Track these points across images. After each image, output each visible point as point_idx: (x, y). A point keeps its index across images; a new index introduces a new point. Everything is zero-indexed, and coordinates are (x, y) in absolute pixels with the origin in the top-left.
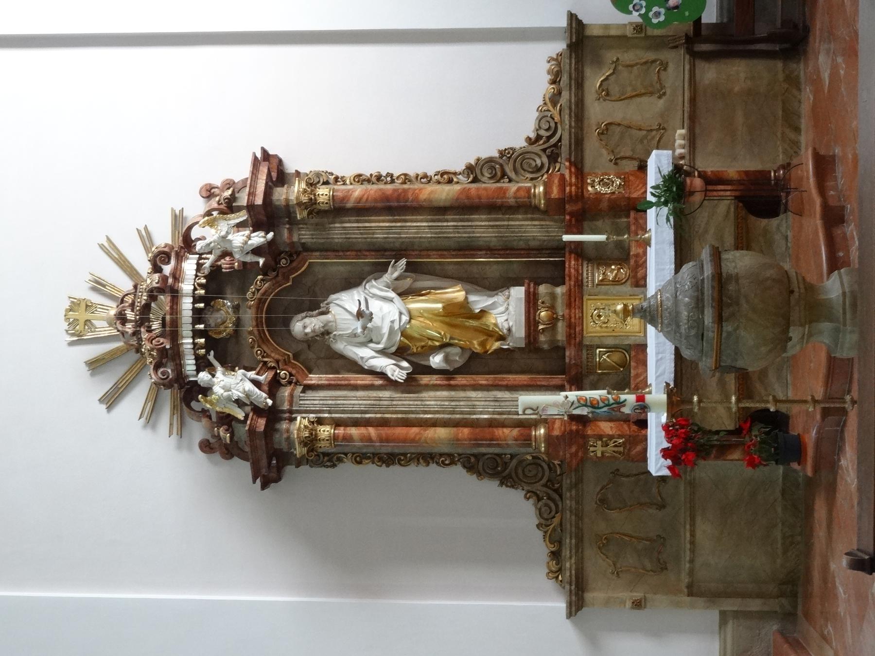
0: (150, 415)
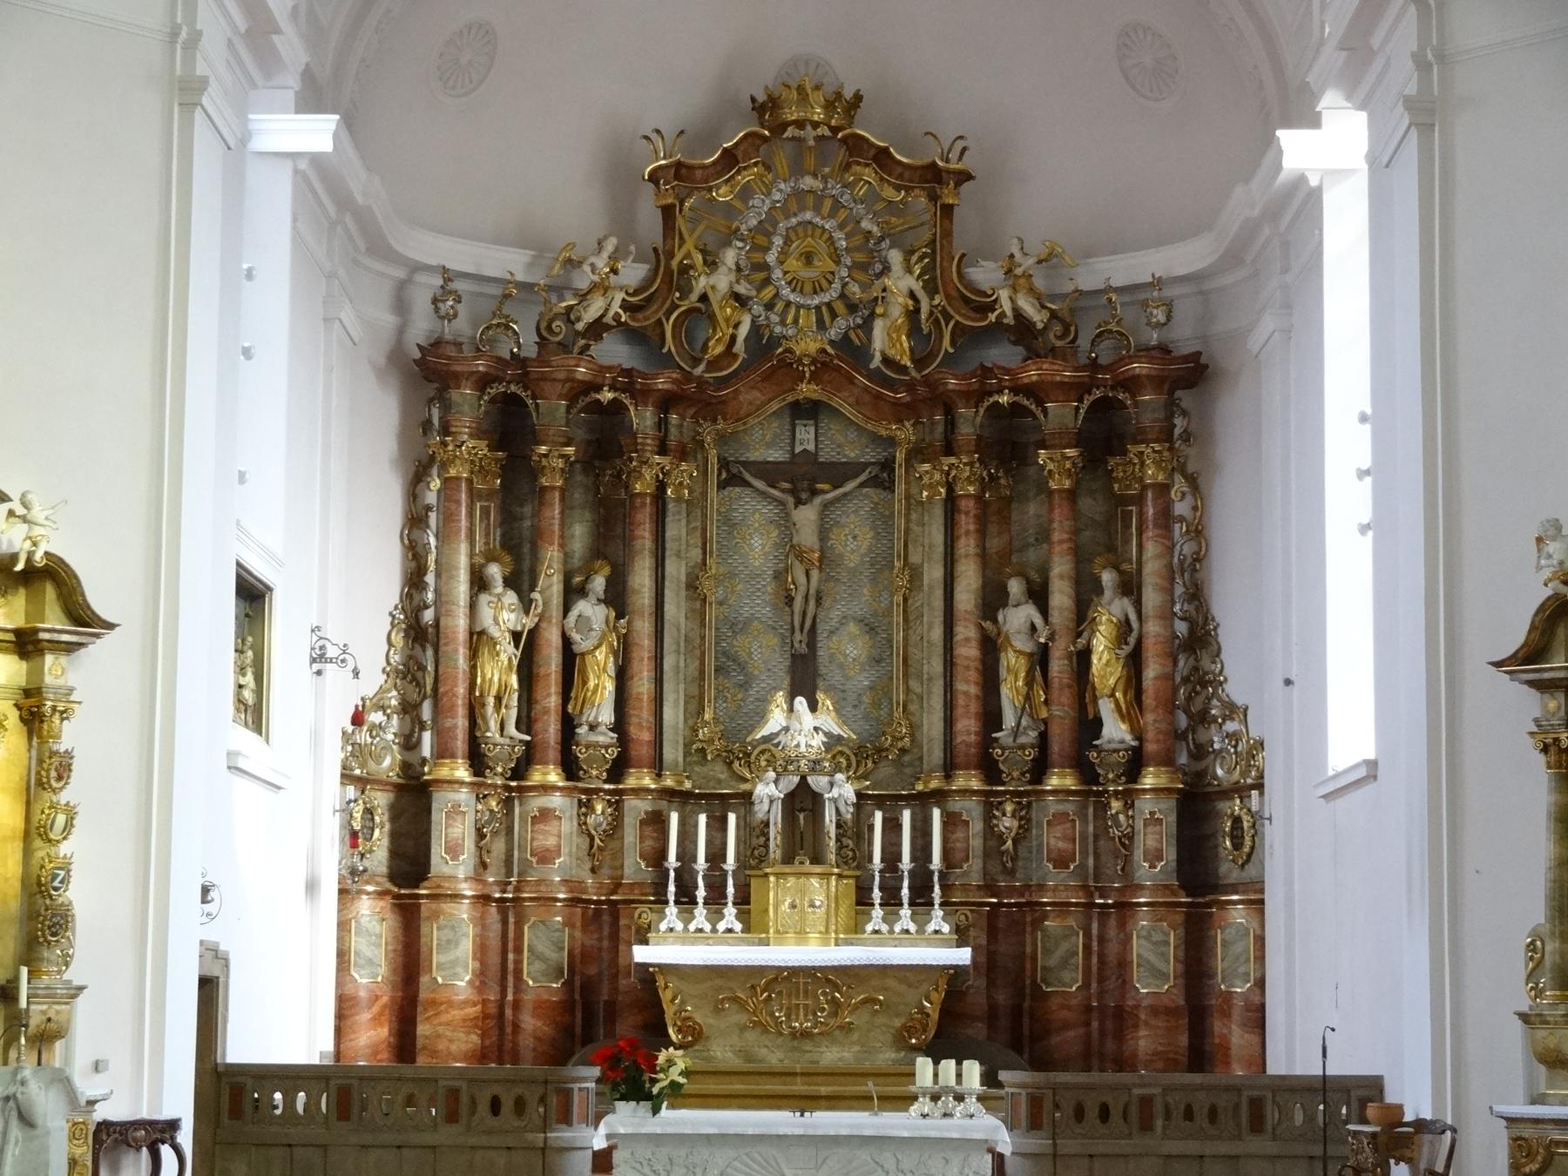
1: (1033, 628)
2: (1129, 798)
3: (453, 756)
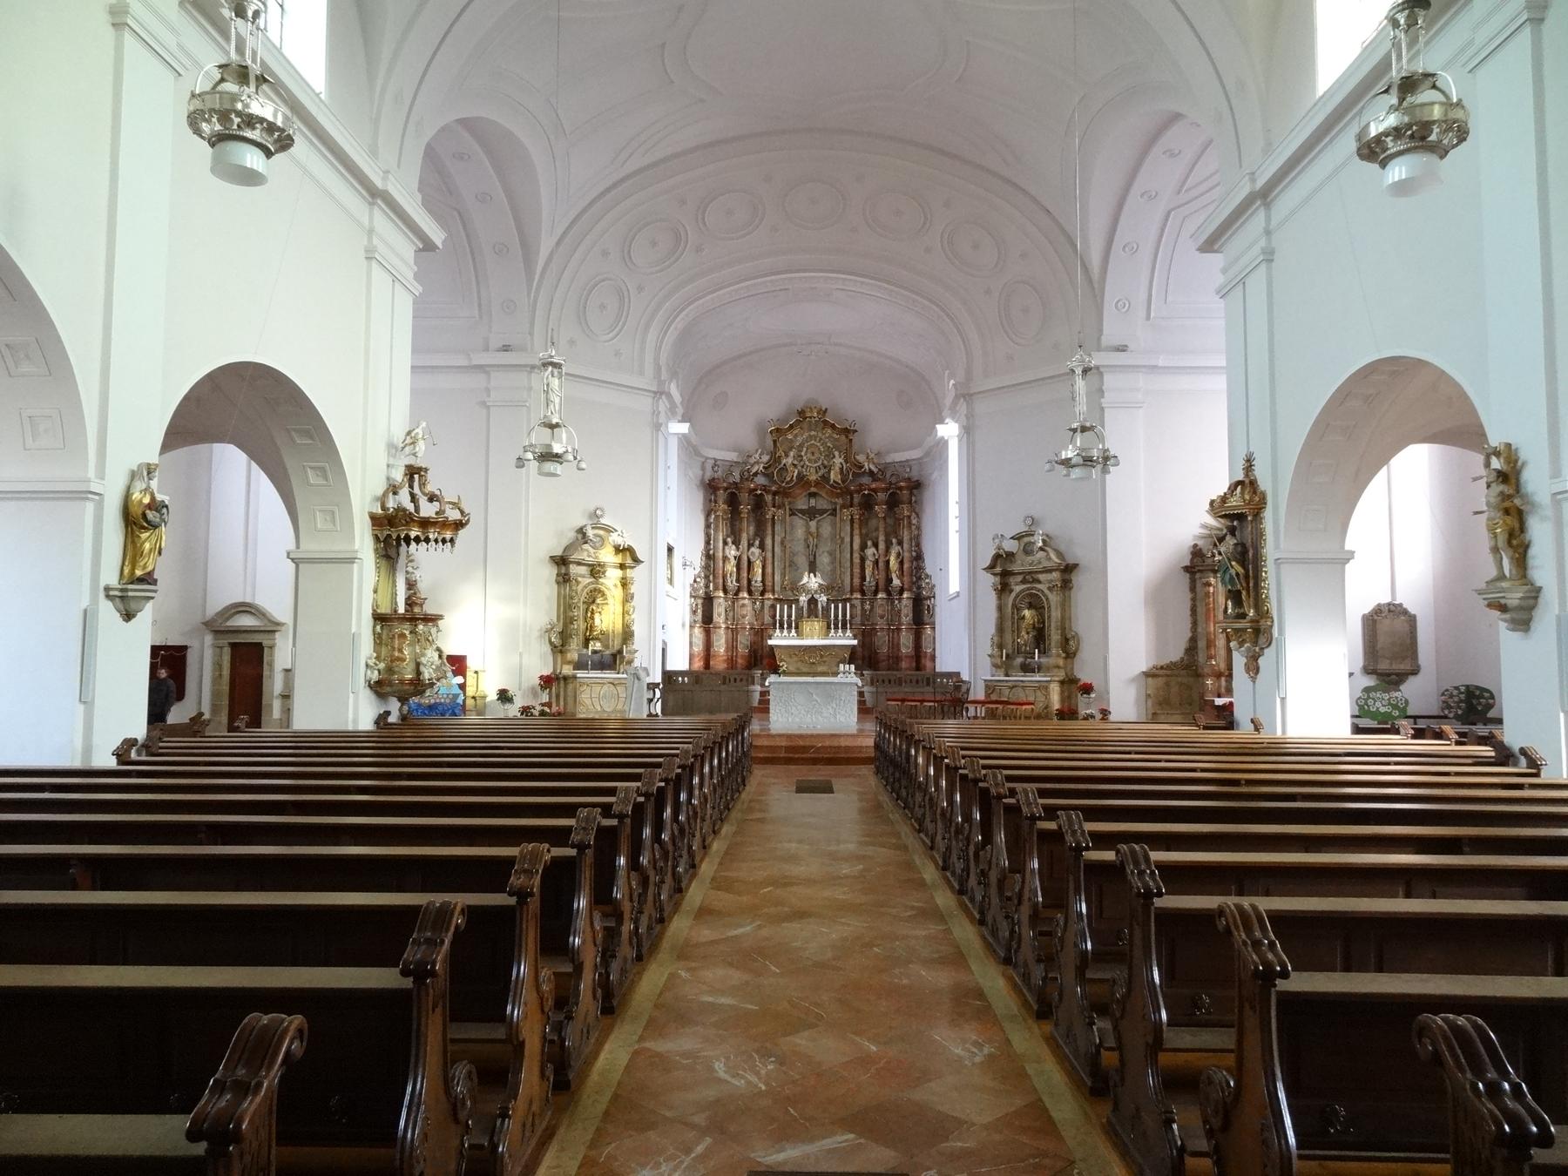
0: (1204, 526)
1: (874, 554)
2: (900, 600)
3: (719, 590)
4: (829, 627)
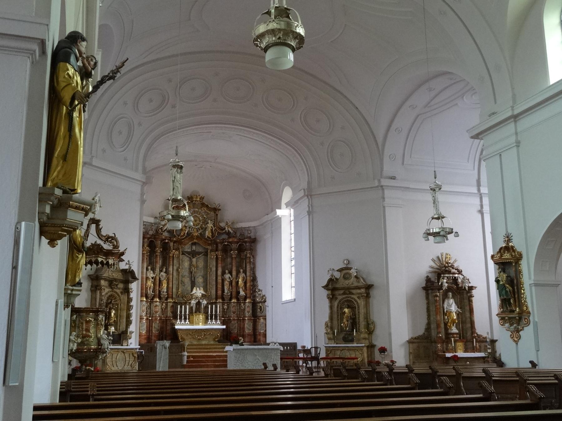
1: (230, 278)
2: (245, 303)
4: (207, 318)
